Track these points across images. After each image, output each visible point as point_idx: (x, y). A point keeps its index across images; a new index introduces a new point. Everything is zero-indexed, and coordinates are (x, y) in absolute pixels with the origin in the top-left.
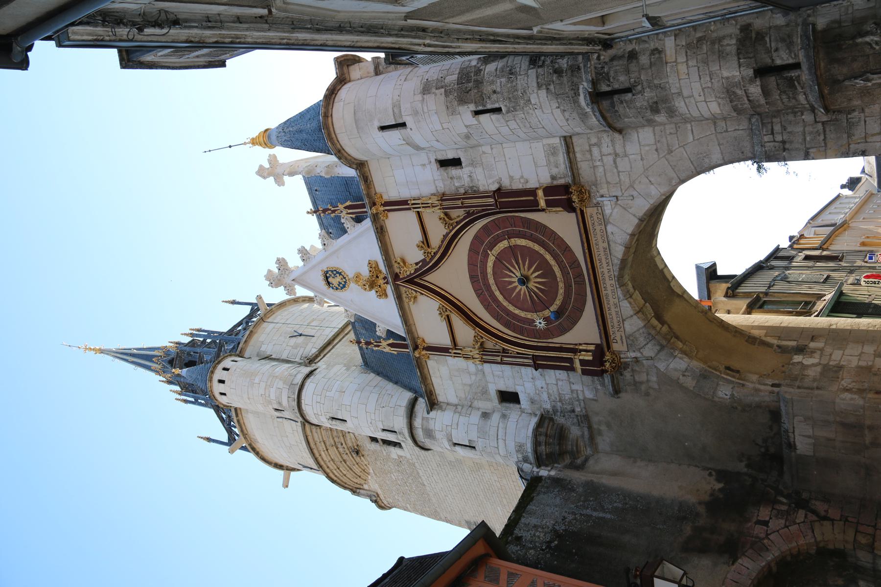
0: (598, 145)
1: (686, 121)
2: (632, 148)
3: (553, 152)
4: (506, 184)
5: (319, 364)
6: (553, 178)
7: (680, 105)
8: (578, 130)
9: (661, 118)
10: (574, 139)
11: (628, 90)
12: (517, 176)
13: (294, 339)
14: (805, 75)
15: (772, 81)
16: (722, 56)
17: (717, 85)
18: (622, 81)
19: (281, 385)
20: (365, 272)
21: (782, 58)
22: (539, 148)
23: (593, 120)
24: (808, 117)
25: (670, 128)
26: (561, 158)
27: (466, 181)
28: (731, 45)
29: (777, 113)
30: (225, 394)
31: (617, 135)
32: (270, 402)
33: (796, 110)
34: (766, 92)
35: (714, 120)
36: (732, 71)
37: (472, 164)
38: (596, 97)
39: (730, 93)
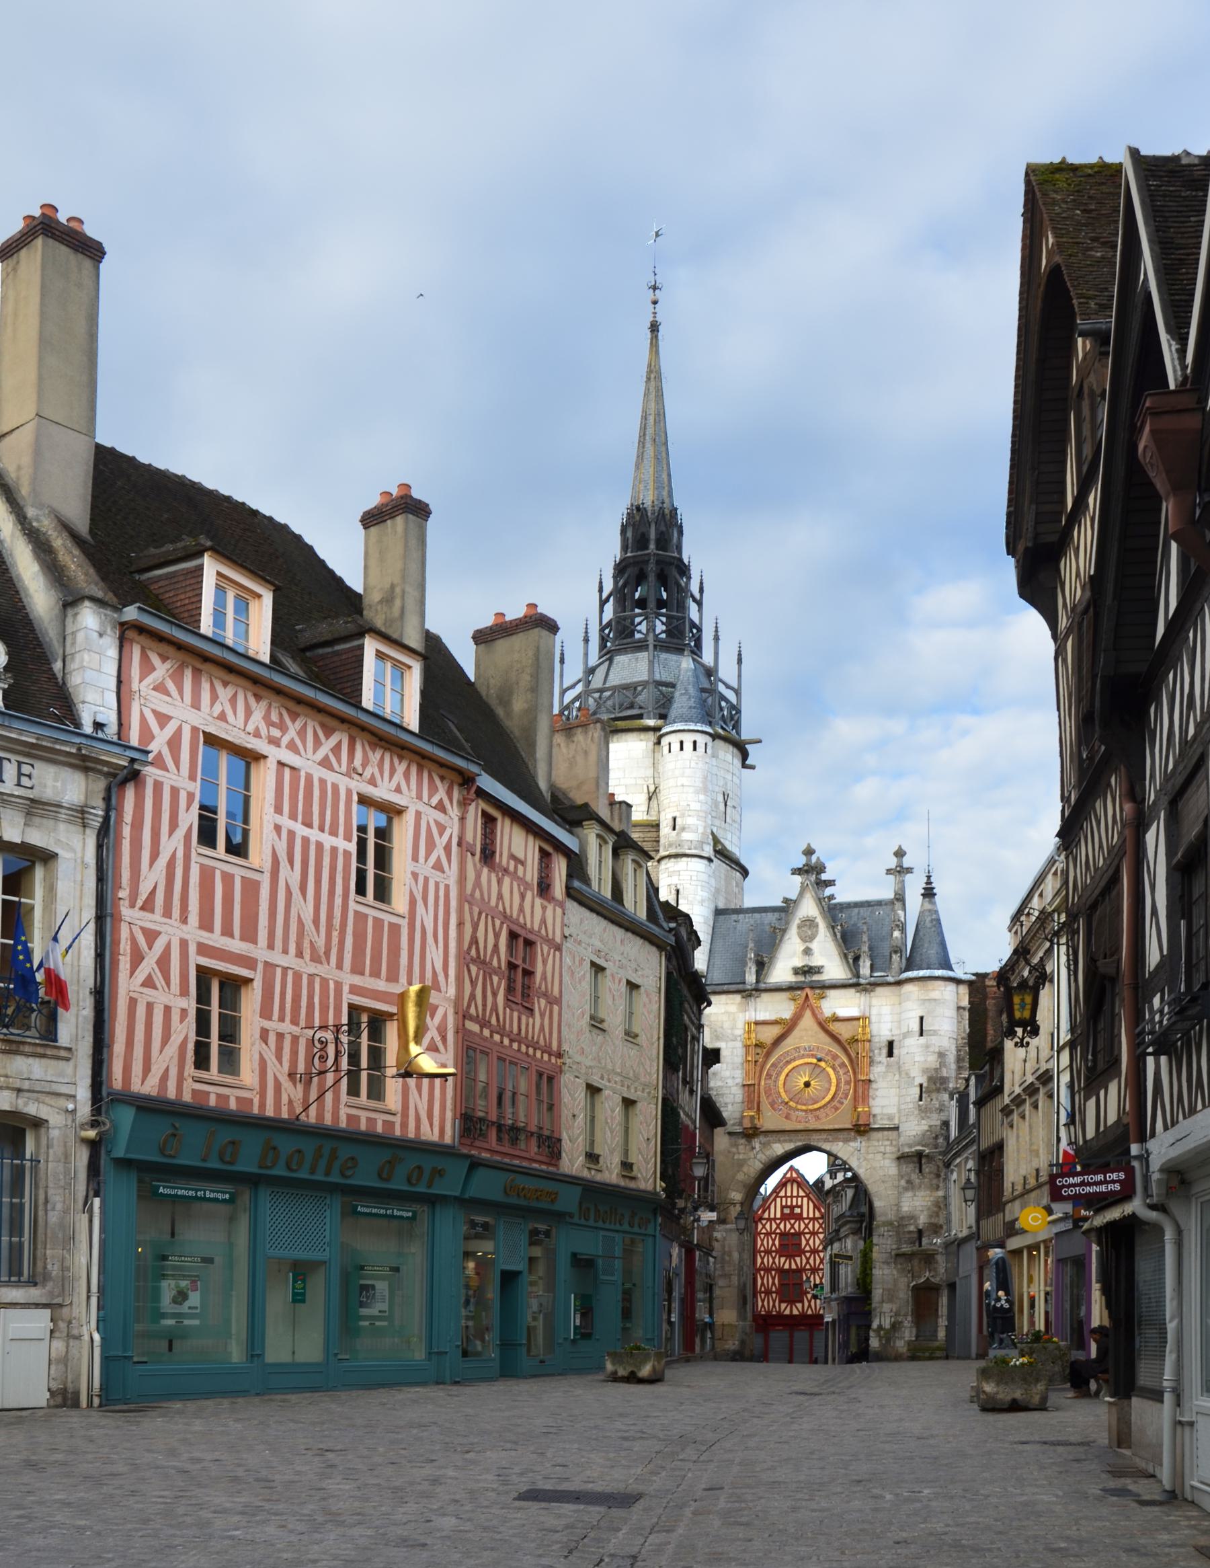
0: (891, 1145)
1: (900, 1193)
2: (887, 1163)
3: (890, 1118)
4: (874, 1086)
5: (715, 860)
6: (874, 1116)
7: (910, 1194)
8: (902, 1139)
9: (903, 1183)
10: (895, 1133)
11: (920, 1171)
12: (878, 1093)
13: (721, 798)
14: (916, 1248)
15: (916, 1235)
16: (931, 1216)
17: (917, 1213)
18: (926, 1169)
19: (701, 830)
20: (816, 961)
21: (925, 1241)
22: (893, 1110)
23: (907, 1150)
24: (894, 1247)
25: (896, 1183)
26: (886, 1123)
27: (877, 1059)
28: (934, 1220)
29: (898, 1233)
30: (682, 749)
31: (895, 1156)
32: (683, 816)
33: (899, 1241)
34: (910, 1232)
35: (898, 1205)
36: (923, 1220)
37: (888, 1065)
38: (919, 1155)
39: (912, 1217)
